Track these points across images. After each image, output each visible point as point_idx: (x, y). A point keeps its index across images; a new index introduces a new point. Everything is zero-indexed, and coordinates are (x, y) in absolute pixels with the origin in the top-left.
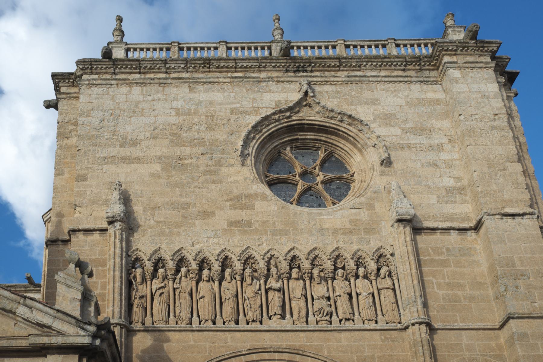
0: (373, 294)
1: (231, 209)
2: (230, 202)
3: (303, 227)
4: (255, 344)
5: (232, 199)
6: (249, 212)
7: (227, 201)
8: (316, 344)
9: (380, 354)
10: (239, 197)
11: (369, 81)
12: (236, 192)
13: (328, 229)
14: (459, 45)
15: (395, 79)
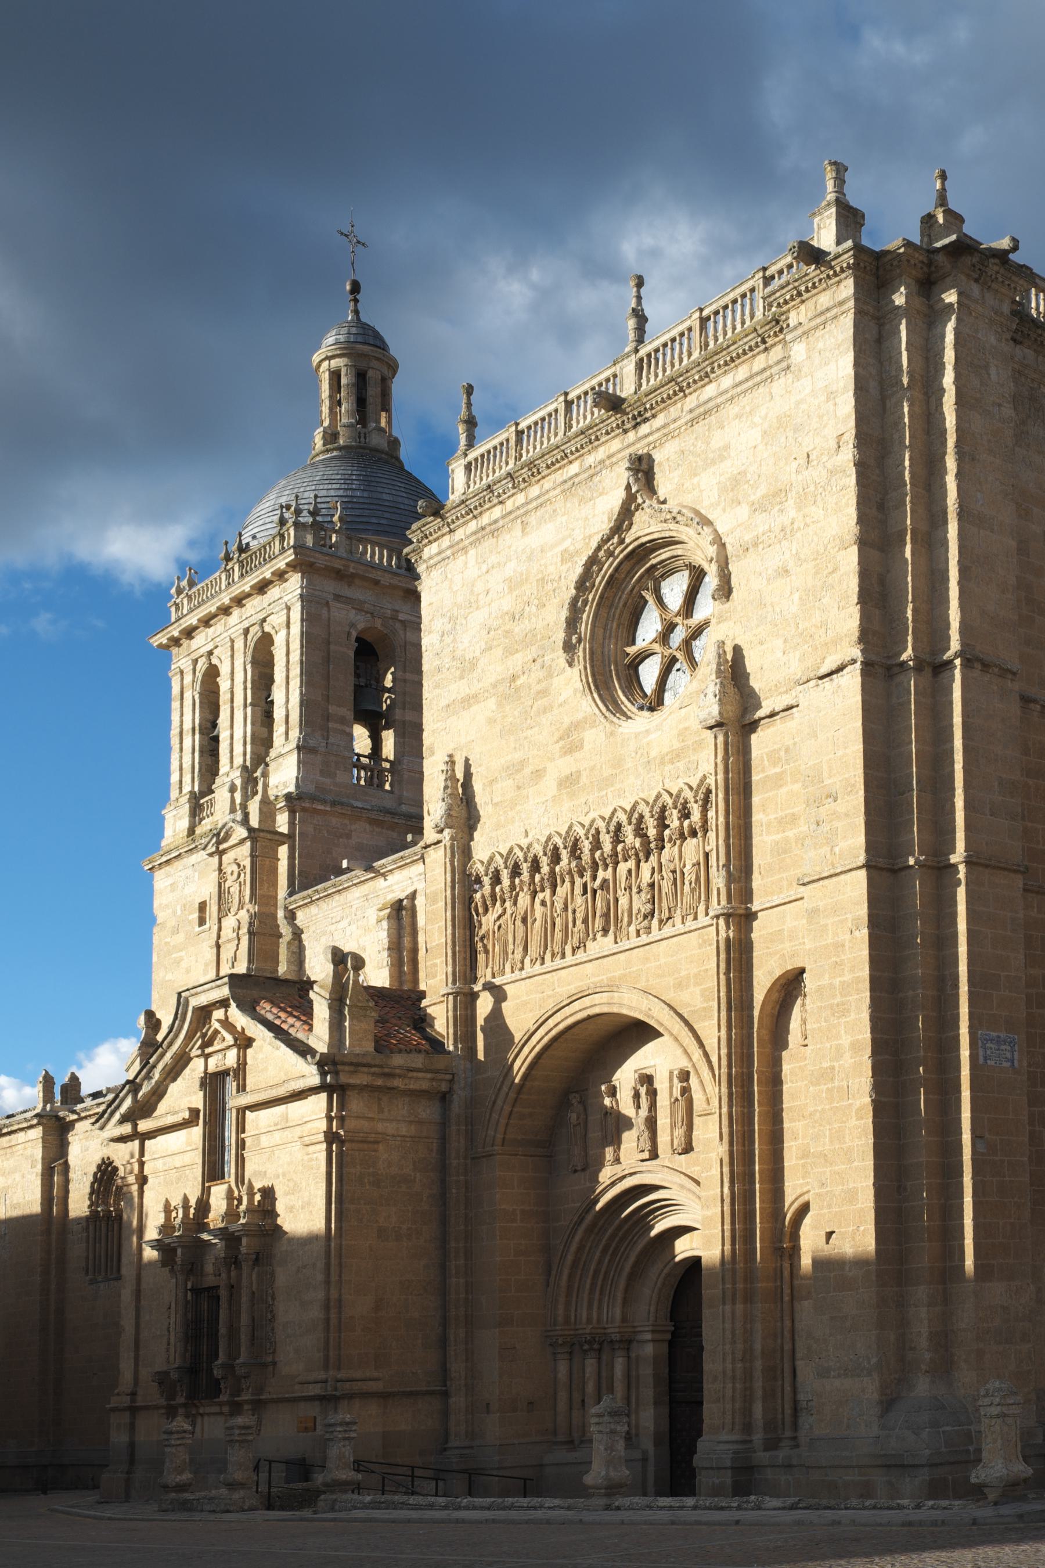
0: (699, 864)
1: (561, 757)
2: (561, 743)
3: (630, 765)
4: (581, 984)
5: (561, 738)
6: (578, 755)
7: (557, 742)
8: (634, 969)
9: (696, 970)
10: (567, 733)
11: (718, 406)
12: (567, 721)
13: (655, 758)
14: (796, 284)
15: (750, 383)
